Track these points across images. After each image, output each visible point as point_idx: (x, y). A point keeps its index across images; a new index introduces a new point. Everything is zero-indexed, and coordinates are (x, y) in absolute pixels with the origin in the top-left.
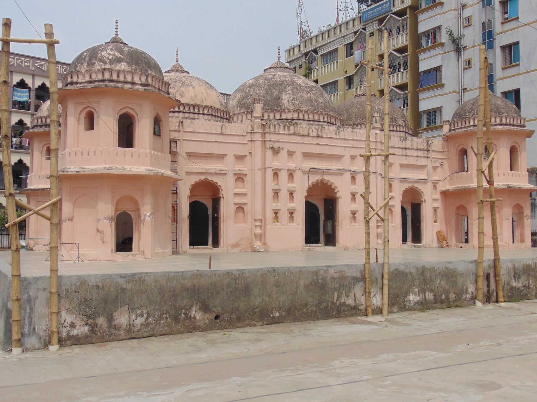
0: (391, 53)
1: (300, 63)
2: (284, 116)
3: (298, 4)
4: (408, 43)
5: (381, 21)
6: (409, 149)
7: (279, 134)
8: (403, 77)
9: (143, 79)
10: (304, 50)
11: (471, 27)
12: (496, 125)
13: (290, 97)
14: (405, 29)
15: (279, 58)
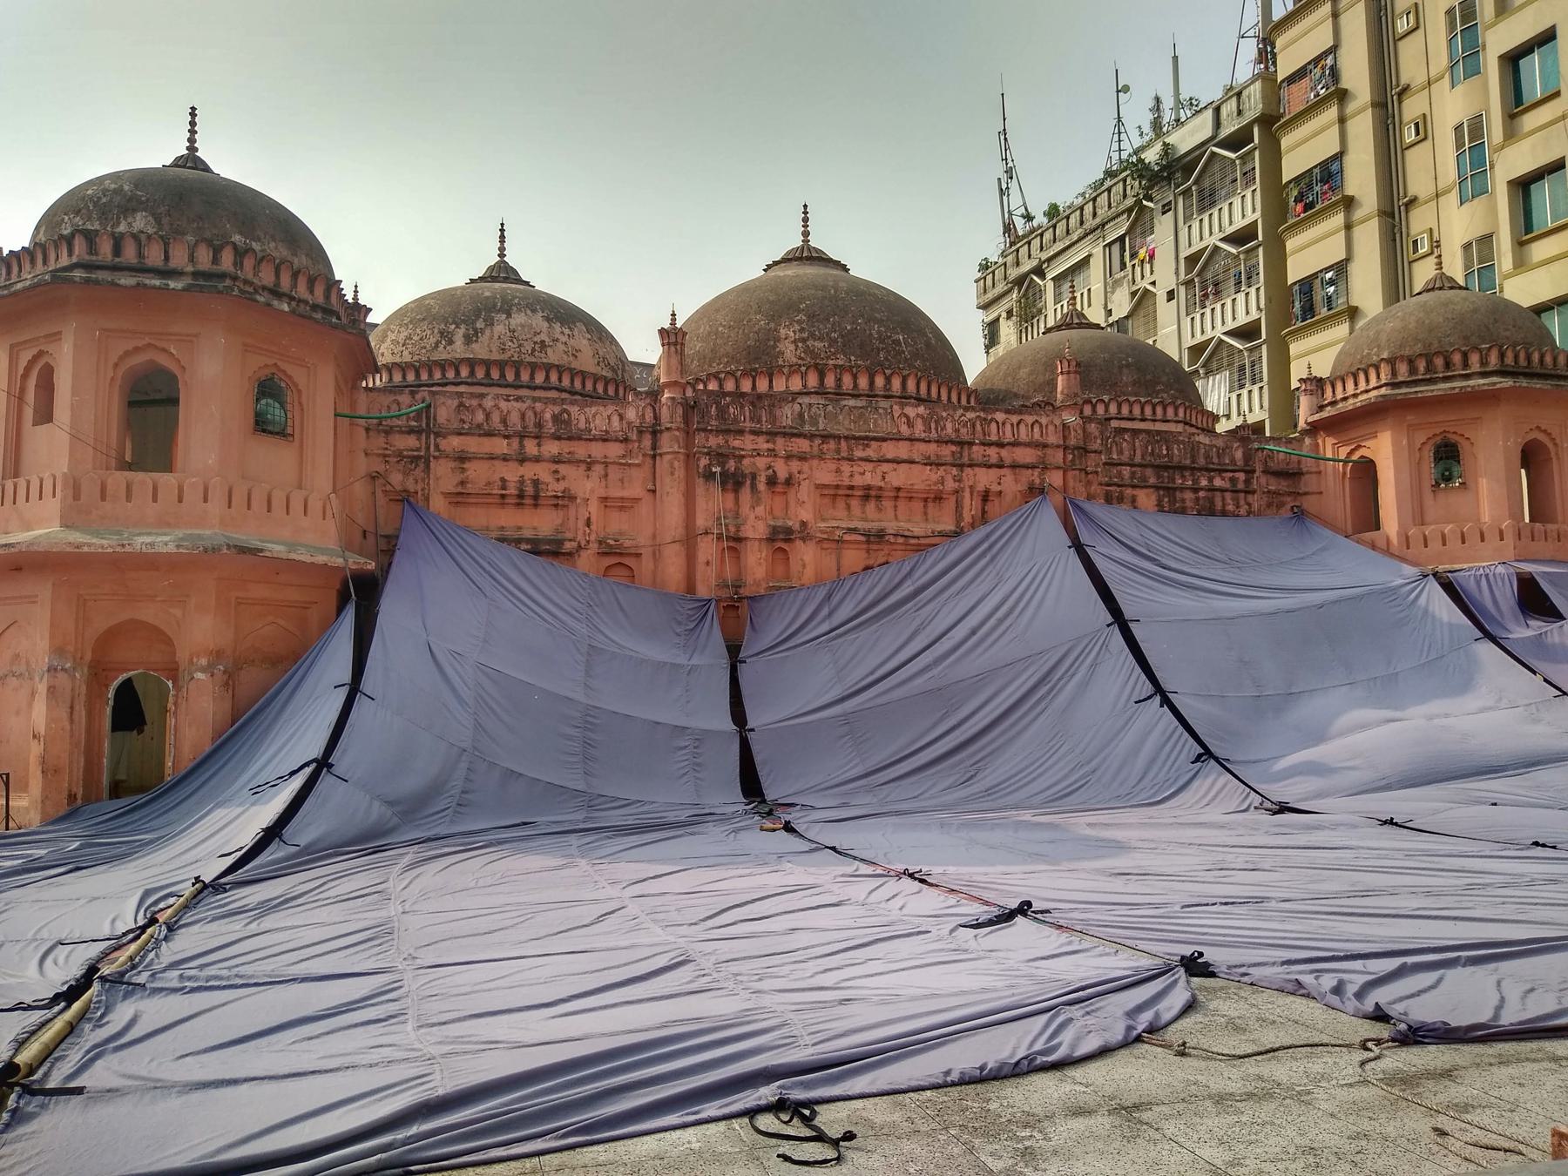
0: (1216, 248)
1: (1006, 307)
2: (780, 385)
3: (1001, 167)
4: (1258, 214)
5: (1188, 169)
6: (1181, 468)
7: (741, 432)
8: (1245, 306)
9: (204, 258)
10: (1014, 273)
11: (1428, 143)
12: (1467, 377)
13: (802, 330)
14: (1248, 177)
15: (806, 234)
